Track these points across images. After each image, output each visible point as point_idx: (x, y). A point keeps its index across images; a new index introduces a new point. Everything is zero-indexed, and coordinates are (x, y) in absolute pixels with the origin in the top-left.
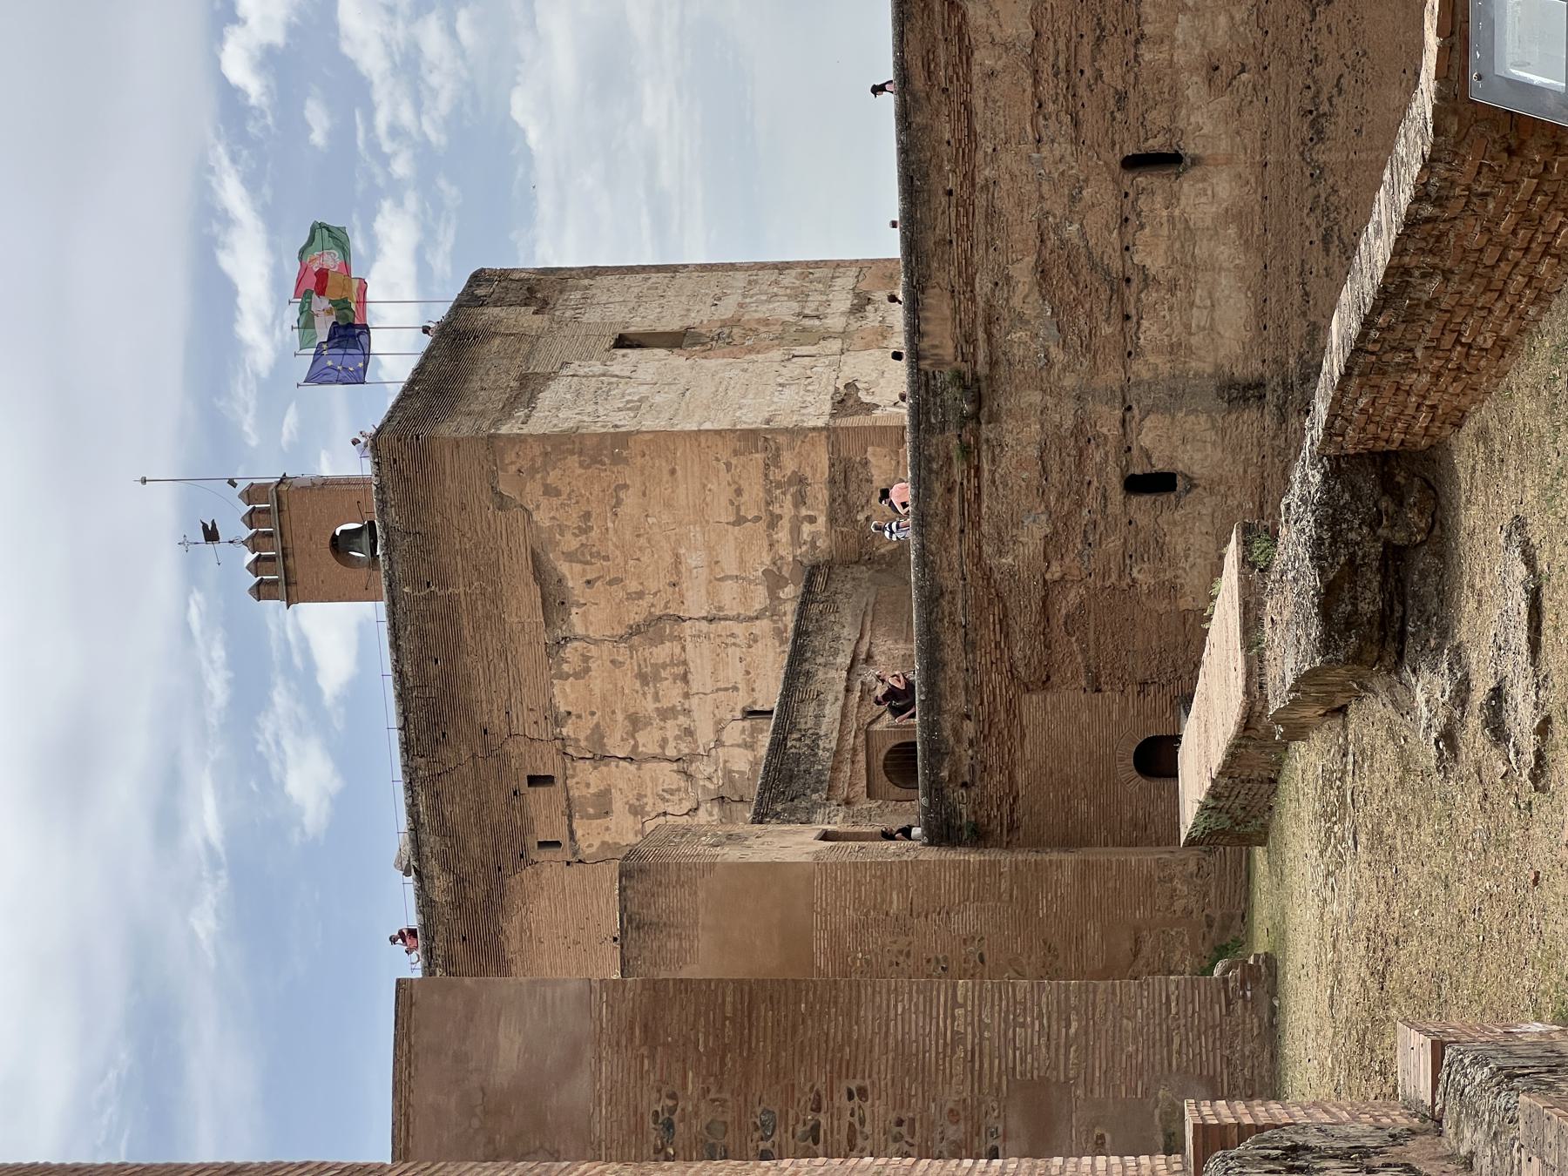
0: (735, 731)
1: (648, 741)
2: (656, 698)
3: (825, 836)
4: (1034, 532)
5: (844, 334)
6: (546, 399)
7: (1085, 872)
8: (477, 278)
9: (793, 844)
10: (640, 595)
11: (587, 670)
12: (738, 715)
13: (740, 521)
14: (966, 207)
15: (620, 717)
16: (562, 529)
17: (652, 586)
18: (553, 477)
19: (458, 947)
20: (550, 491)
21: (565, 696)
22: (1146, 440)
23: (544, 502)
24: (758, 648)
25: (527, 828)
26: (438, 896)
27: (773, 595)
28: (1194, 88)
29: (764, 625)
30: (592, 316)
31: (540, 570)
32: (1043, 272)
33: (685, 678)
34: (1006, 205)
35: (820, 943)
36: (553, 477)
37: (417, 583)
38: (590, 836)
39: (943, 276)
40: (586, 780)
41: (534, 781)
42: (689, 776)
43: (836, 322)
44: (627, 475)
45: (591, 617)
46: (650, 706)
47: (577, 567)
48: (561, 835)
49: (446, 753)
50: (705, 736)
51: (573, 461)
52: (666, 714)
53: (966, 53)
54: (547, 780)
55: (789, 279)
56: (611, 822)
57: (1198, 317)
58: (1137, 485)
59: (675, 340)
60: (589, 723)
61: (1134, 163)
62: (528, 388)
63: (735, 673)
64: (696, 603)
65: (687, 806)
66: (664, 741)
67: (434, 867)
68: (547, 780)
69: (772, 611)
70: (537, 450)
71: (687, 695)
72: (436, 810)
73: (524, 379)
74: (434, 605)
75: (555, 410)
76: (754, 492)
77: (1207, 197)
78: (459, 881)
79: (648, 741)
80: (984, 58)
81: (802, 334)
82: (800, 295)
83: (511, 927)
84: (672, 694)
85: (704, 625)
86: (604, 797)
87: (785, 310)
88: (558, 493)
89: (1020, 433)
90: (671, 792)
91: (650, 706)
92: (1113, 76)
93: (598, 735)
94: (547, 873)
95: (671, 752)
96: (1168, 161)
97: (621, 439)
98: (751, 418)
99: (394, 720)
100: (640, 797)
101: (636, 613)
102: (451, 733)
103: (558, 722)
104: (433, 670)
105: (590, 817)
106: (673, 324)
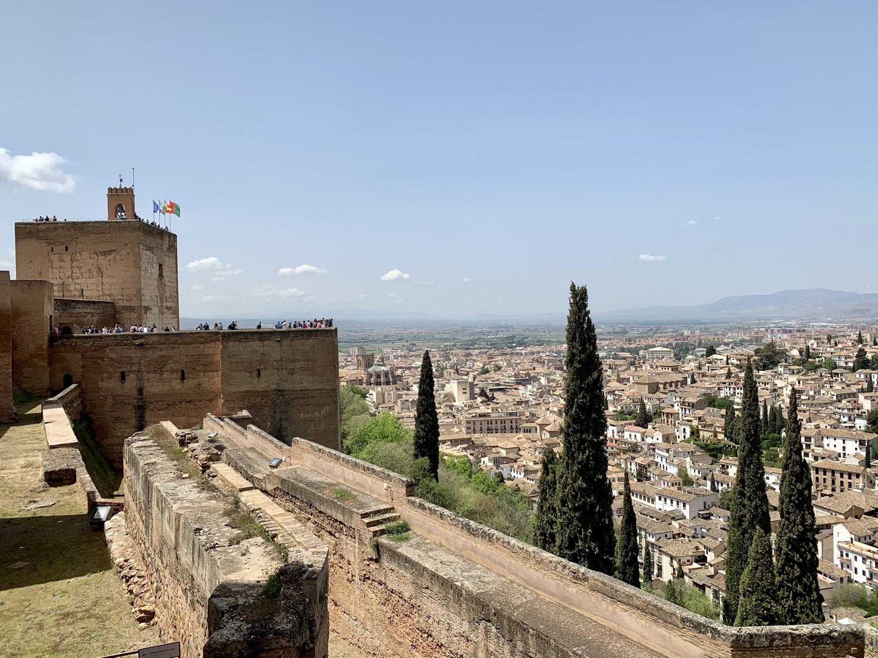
1: (75, 270)
3: (51, 316)
4: (112, 355)
5: (162, 306)
6: (148, 253)
7: (44, 367)
8: (175, 236)
9: (49, 310)
14: (175, 343)
22: (131, 375)
28: (196, 381)
30: (166, 259)
31: (112, 251)
32: (163, 356)
34: (175, 350)
35: (27, 318)
38: (55, 258)
39: (162, 339)
40: (67, 257)
41: (67, 248)
43: (165, 304)
46: (83, 270)
50: (77, 281)
52: (82, 274)
53: (203, 343)
54: (67, 250)
55: (174, 294)
57: (155, 383)
58: (123, 374)
59: (161, 275)
61: (183, 372)
62: (149, 249)
63: (91, 287)
68: (67, 250)
73: (153, 248)
75: (145, 254)
76: (126, 292)
77: (177, 384)
79: (75, 270)
80: (202, 346)
81: (162, 298)
82: (171, 297)
84: (85, 275)
87: (168, 294)
89: (133, 353)
92: (198, 368)
96: (183, 378)
97: (139, 268)
98: (143, 292)
99: (80, 220)
106: (164, 274)
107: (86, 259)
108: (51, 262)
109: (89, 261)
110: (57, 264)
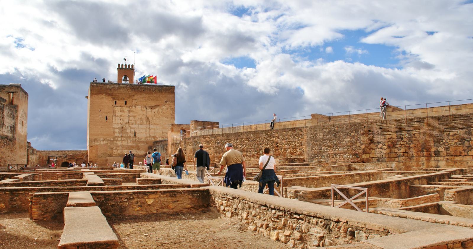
0: (133, 131)
1: (131, 118)
2: (138, 120)
10: (153, 119)
11: (142, 111)
12: (135, 131)
13: (163, 133)
15: (135, 115)
16: (162, 109)
17: (154, 121)
18: (169, 109)
19: (100, 88)
20: (167, 109)
21: (139, 107)
23: (166, 108)
24: (145, 134)
25: (118, 100)
26: (108, 86)
27: (152, 137)
29: (148, 135)
31: (156, 106)
33: (141, 124)
36: (169, 109)
37: (155, 89)
38: (117, 109)
40: (126, 109)
41: (126, 103)
42: (126, 123)
44: (169, 119)
45: (150, 112)
46: (137, 119)
47: (157, 111)
48: (117, 105)
49: (130, 90)
51: (171, 112)
52: (136, 121)
56: (119, 112)
60: (135, 110)
64: (151, 126)
65: (122, 123)
66: (132, 121)
67: (113, 86)
69: (150, 137)
70: (173, 107)
71: (138, 124)
72: (121, 88)
74: (152, 91)
78: (110, 89)
79: (131, 118)
83: (103, 96)
85: (148, 127)
86: (123, 111)
88: (167, 109)
90: (124, 121)
91: (137, 119)
93: (132, 111)
94: (111, 102)
95: (130, 121)
100: (123, 116)
101: (150, 118)
102: (133, 91)
103: (135, 106)
104: (143, 90)
105: (120, 109)
107: (139, 110)
108: (114, 112)
109: (141, 112)
110: (118, 113)
